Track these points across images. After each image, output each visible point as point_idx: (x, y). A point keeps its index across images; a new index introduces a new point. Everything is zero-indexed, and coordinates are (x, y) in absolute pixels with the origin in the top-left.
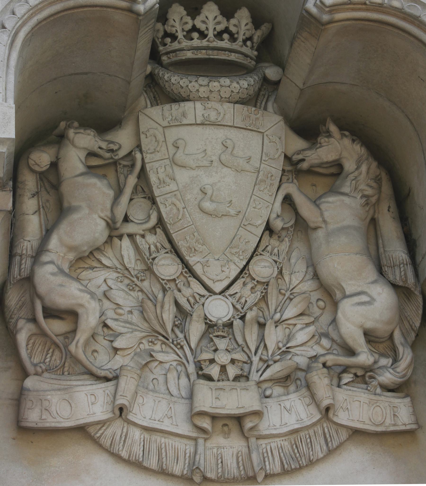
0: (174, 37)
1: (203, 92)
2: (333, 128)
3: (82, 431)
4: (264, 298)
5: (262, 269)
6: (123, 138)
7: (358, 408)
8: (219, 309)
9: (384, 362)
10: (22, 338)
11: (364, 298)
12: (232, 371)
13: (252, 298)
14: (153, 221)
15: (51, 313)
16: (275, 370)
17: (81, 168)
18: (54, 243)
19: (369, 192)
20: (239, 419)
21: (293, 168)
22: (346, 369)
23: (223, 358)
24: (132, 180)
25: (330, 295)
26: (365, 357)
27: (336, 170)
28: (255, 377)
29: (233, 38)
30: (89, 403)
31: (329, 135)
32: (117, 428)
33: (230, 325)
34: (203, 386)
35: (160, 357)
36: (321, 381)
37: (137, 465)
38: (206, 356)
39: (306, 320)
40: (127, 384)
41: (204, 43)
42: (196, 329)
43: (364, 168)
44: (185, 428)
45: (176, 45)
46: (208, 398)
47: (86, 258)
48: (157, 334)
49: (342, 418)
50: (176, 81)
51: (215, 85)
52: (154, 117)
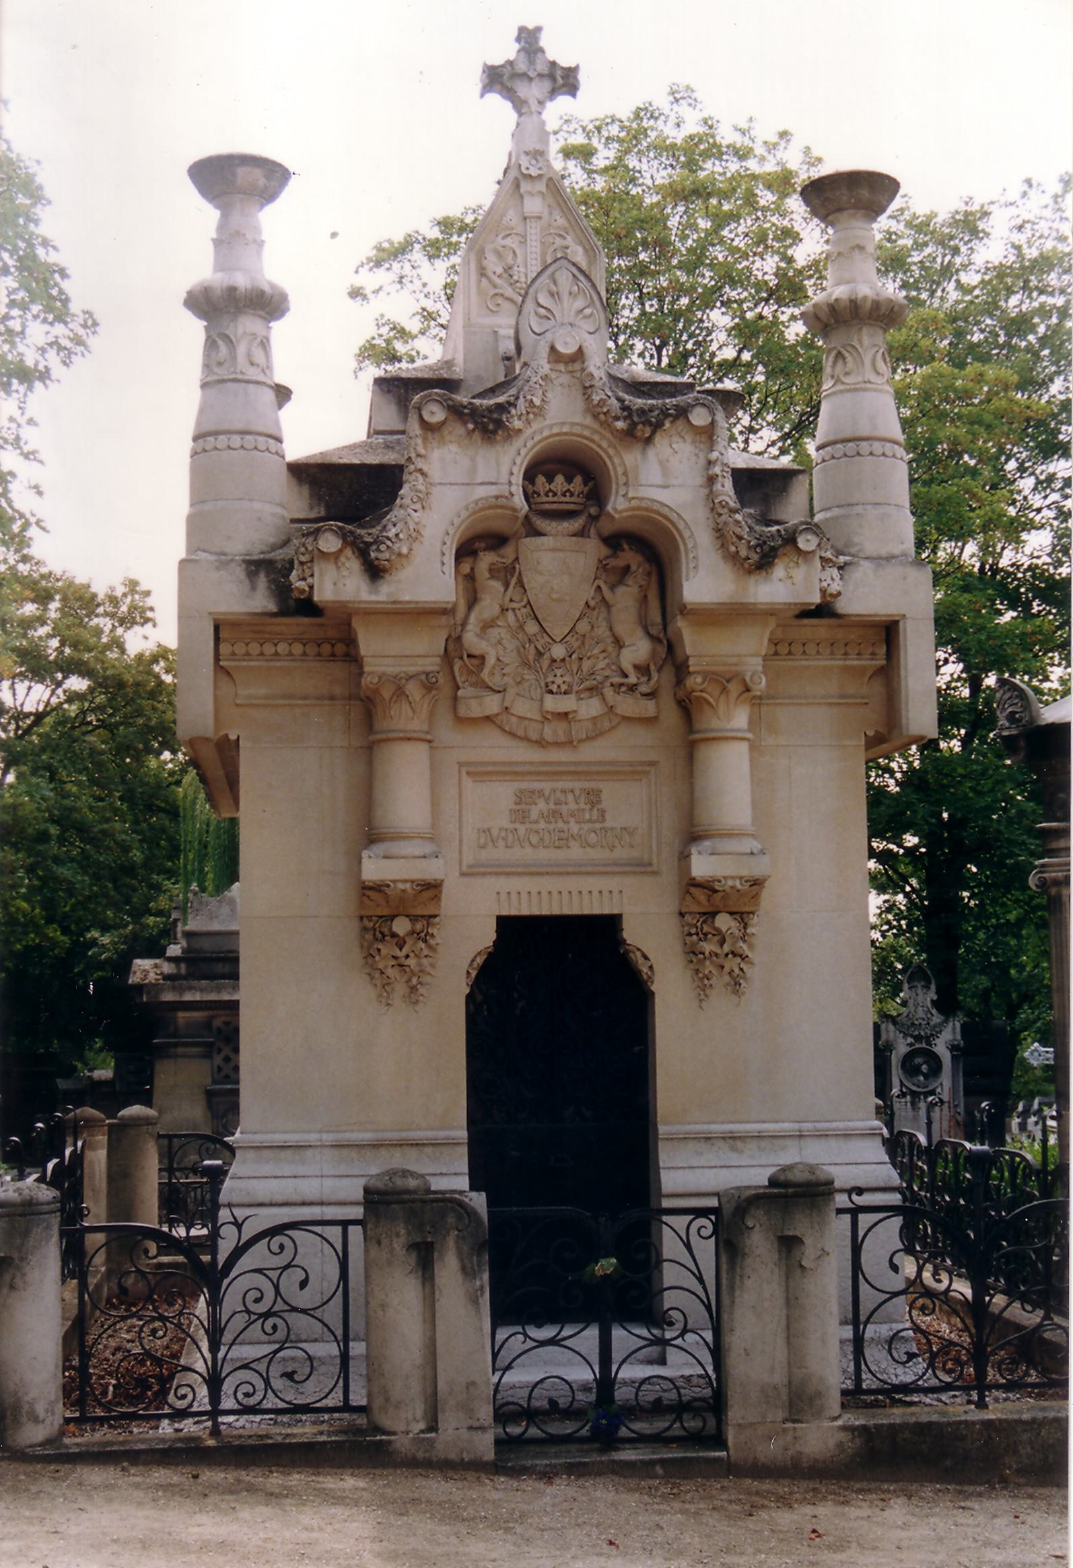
0: (539, 495)
1: (553, 532)
2: (625, 546)
3: (488, 719)
4: (583, 643)
5: (583, 627)
6: (509, 551)
7: (628, 705)
8: (558, 651)
9: (644, 679)
10: (456, 668)
11: (634, 648)
12: (564, 688)
13: (576, 645)
14: (525, 600)
15: (469, 656)
16: (587, 684)
17: (487, 575)
18: (473, 618)
19: (643, 583)
20: (566, 714)
21: (603, 566)
22: (622, 685)
23: (559, 681)
24: (513, 581)
25: (619, 643)
26: (633, 679)
27: (626, 570)
28: (575, 688)
29: (572, 495)
30: (492, 704)
31: (623, 550)
32: (504, 717)
33: (563, 660)
34: (548, 697)
35: (526, 677)
36: (608, 692)
37: (513, 735)
38: (550, 679)
39: (604, 655)
40: (511, 692)
41: (555, 499)
42: (545, 662)
43: (641, 570)
44: (539, 718)
45: (539, 500)
46: (551, 703)
47: (487, 626)
48: (525, 664)
49: (619, 711)
50: (541, 523)
51: (560, 528)
52: (529, 543)
